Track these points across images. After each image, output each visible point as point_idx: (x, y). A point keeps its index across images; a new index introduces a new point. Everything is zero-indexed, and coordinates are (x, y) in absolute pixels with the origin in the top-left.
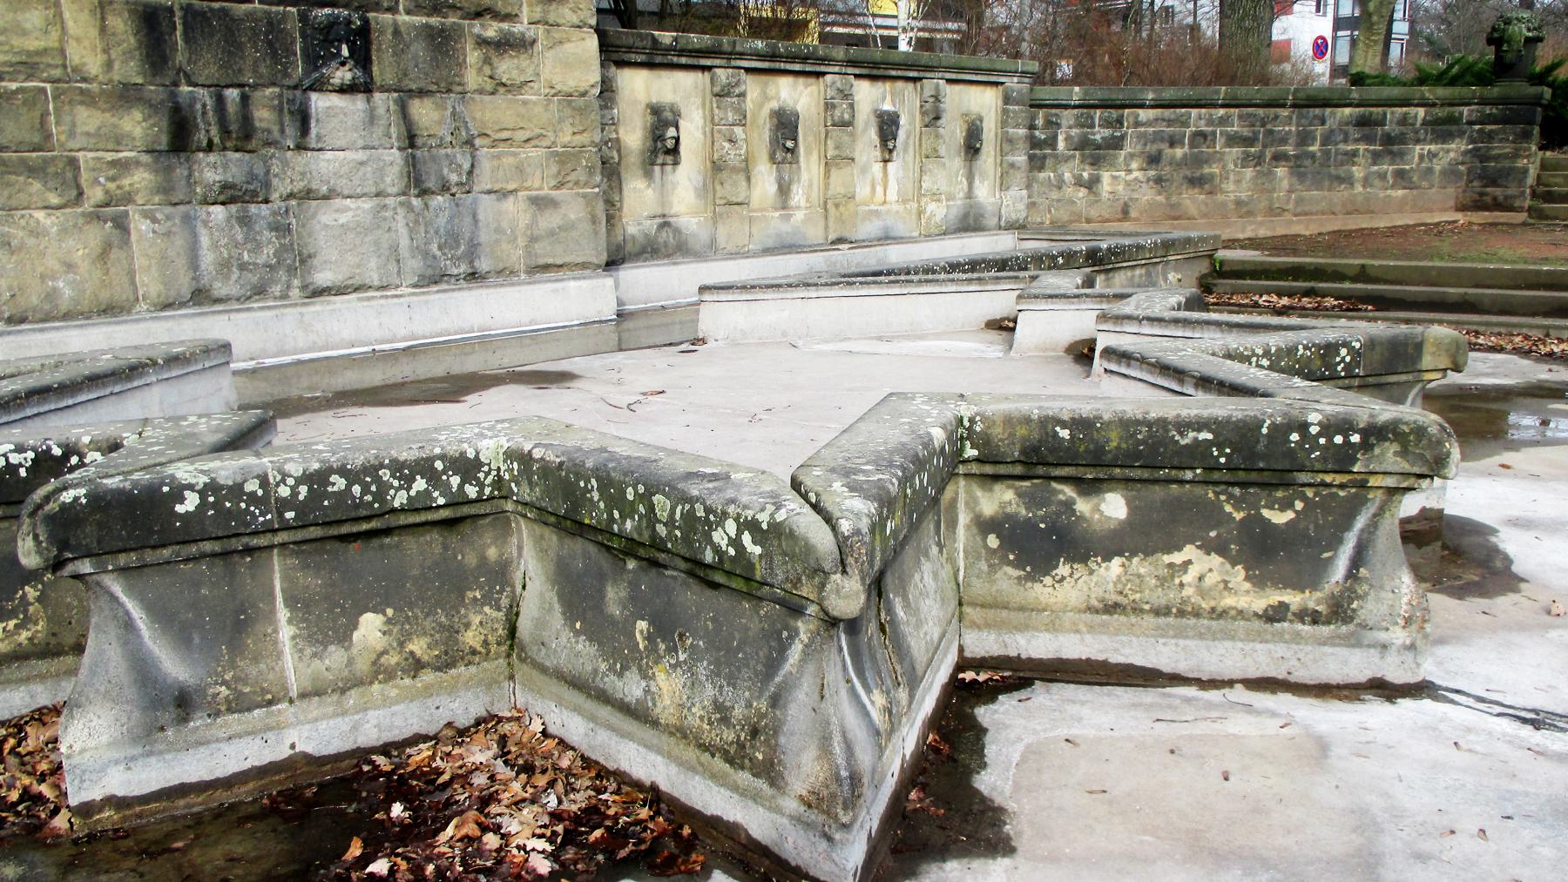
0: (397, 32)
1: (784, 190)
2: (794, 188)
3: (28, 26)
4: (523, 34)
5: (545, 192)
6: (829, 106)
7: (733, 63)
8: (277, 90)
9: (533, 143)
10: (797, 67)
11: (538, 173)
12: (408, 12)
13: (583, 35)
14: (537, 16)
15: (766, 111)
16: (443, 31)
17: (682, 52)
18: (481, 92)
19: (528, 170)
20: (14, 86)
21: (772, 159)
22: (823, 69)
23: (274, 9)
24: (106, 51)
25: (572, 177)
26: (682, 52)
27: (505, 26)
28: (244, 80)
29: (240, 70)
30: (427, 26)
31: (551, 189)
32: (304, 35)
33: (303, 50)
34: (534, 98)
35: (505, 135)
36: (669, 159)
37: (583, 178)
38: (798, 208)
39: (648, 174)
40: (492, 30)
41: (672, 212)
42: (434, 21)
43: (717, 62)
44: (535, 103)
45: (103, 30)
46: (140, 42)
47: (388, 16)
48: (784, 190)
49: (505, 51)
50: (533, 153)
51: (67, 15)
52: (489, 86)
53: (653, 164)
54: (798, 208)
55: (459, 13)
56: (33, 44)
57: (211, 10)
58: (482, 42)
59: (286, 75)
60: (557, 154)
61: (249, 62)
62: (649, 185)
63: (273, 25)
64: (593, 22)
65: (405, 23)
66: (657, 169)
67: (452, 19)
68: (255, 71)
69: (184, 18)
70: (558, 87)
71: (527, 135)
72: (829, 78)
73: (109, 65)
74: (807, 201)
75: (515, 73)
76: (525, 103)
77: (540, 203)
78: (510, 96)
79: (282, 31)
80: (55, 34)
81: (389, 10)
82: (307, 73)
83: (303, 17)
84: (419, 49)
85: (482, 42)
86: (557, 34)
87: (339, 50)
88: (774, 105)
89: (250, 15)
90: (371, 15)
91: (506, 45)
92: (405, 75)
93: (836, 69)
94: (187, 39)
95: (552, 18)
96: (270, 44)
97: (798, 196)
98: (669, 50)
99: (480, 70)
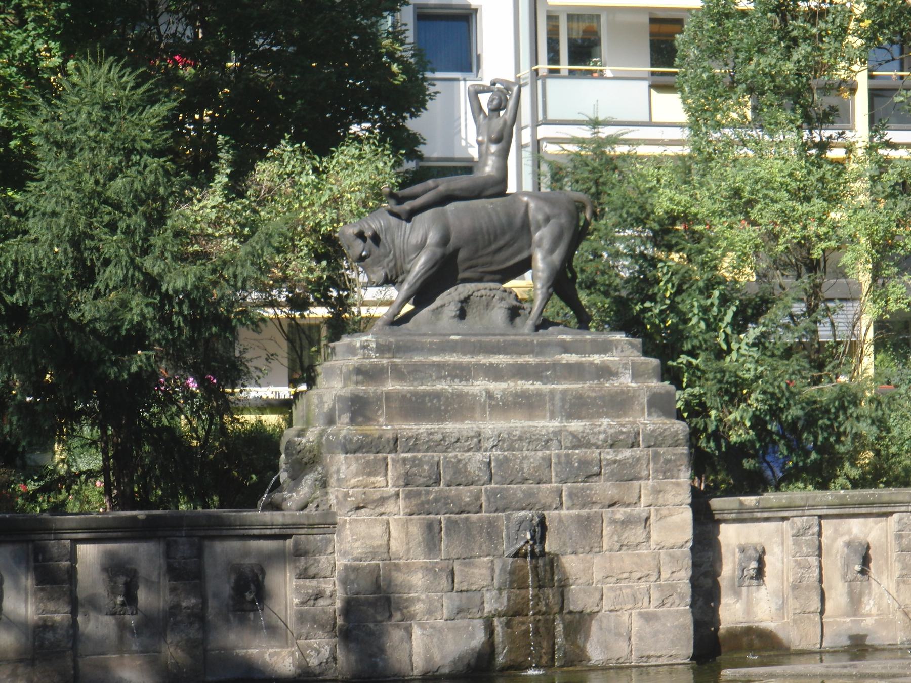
0: (560, 520)
1: (855, 601)
2: (865, 599)
3: (374, 535)
4: (639, 514)
5: (652, 609)
6: (899, 537)
7: (807, 513)
8: (491, 558)
9: (643, 580)
10: (864, 510)
11: (646, 599)
12: (568, 509)
13: (681, 511)
14: (649, 502)
15: (840, 543)
16: (588, 517)
17: (764, 509)
18: (611, 550)
19: (639, 596)
20: (366, 563)
21: (844, 577)
22: (890, 510)
23: (492, 514)
24: (408, 544)
25: (670, 600)
26: (764, 509)
27: (628, 510)
28: (474, 554)
29: (473, 549)
30: (579, 516)
31: (656, 607)
32: (507, 528)
33: (508, 536)
34: (646, 552)
35: (626, 575)
36: (754, 582)
37: (677, 601)
38: (869, 615)
39: (737, 594)
40: (620, 513)
41: (756, 619)
42: (584, 512)
43: (795, 513)
44: (646, 556)
45: (407, 533)
46: (424, 539)
47: (556, 512)
48: (855, 601)
49: (627, 526)
50: (643, 585)
51: (391, 528)
52: (617, 546)
53: (740, 586)
54: (869, 615)
55: (600, 506)
56: (377, 543)
57: (460, 518)
58: (613, 521)
59: (496, 549)
60: (660, 585)
61: (478, 544)
62: (738, 601)
63: (492, 524)
64: (689, 501)
65: (566, 515)
66: (744, 589)
67: (596, 509)
68: (480, 548)
69: (446, 524)
70: (663, 544)
71: (639, 575)
72: (896, 516)
73: (408, 551)
74: (878, 609)
75: (632, 539)
76: (639, 556)
77: (648, 617)
78: (630, 552)
79: (495, 526)
80: (386, 538)
81: (556, 509)
82: (507, 548)
83: (508, 518)
84: (573, 529)
85: (613, 521)
86: (664, 511)
87: (526, 535)
88: (846, 538)
89: (480, 519)
90: (546, 513)
91: (626, 523)
92: (564, 545)
93: (903, 509)
94: (447, 535)
95: (661, 501)
96: (488, 533)
97: (869, 606)
98: (752, 510)
99: (611, 537)
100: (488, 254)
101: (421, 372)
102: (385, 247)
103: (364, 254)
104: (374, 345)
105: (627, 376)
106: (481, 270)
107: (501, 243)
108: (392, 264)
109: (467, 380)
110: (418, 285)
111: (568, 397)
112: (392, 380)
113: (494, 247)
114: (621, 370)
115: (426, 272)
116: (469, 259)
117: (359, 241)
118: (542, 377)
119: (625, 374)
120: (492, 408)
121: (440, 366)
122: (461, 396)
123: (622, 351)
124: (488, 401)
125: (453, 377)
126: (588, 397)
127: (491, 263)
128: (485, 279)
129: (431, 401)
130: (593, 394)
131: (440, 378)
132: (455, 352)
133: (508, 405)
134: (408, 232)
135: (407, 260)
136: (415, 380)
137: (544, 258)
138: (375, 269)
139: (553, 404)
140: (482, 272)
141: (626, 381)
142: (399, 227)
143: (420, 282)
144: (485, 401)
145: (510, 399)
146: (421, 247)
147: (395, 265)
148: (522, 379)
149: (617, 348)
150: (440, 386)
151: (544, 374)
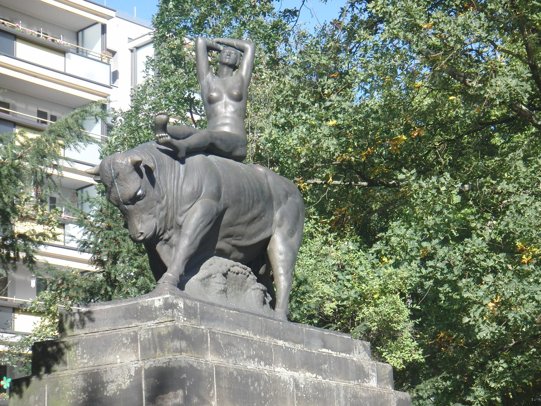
100: (243, 224)
101: (235, 347)
102: (159, 190)
103: (140, 192)
104: (181, 305)
105: (375, 379)
106: (234, 242)
107: (255, 212)
108: (163, 214)
109: (270, 365)
110: (197, 242)
111: (349, 396)
112: (211, 353)
113: (249, 216)
114: (371, 372)
115: (205, 227)
116: (231, 225)
117: (136, 175)
118: (321, 370)
119: (373, 376)
120: (299, 398)
121: (249, 342)
122: (276, 380)
123: (359, 353)
124: (295, 391)
125: (261, 359)
126: (361, 397)
127: (241, 236)
128: (233, 256)
129: (253, 384)
130: (364, 395)
131: (250, 357)
132: (248, 329)
133: (309, 399)
134: (182, 176)
135: (180, 211)
136: (230, 356)
137: (285, 240)
138: (145, 216)
139: (339, 402)
140: (234, 246)
141: (373, 383)
142: (173, 166)
143: (199, 238)
144: (293, 391)
145: (311, 391)
146: (195, 196)
147: (167, 215)
148: (309, 370)
149: (356, 348)
150: (252, 366)
151: (323, 367)
